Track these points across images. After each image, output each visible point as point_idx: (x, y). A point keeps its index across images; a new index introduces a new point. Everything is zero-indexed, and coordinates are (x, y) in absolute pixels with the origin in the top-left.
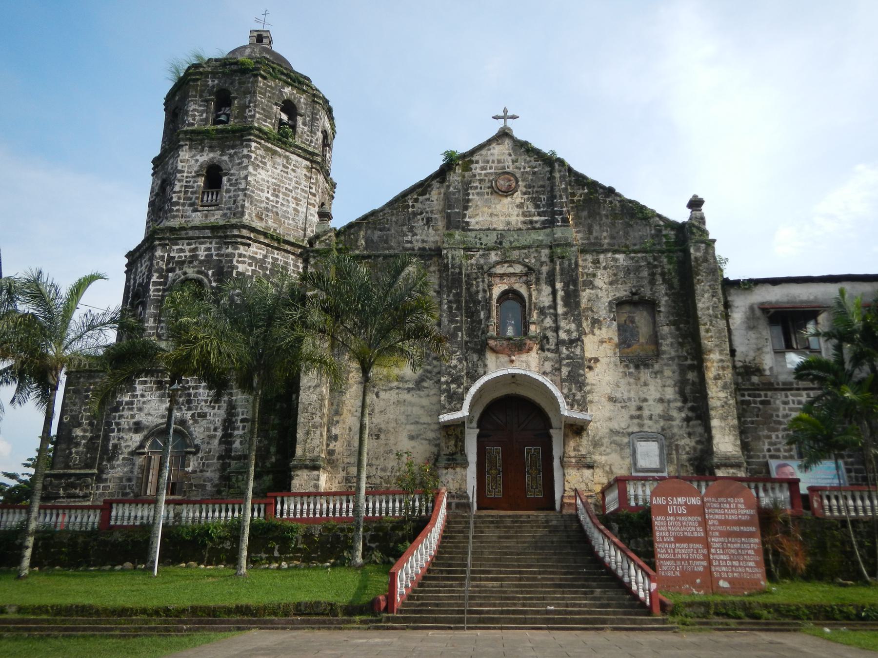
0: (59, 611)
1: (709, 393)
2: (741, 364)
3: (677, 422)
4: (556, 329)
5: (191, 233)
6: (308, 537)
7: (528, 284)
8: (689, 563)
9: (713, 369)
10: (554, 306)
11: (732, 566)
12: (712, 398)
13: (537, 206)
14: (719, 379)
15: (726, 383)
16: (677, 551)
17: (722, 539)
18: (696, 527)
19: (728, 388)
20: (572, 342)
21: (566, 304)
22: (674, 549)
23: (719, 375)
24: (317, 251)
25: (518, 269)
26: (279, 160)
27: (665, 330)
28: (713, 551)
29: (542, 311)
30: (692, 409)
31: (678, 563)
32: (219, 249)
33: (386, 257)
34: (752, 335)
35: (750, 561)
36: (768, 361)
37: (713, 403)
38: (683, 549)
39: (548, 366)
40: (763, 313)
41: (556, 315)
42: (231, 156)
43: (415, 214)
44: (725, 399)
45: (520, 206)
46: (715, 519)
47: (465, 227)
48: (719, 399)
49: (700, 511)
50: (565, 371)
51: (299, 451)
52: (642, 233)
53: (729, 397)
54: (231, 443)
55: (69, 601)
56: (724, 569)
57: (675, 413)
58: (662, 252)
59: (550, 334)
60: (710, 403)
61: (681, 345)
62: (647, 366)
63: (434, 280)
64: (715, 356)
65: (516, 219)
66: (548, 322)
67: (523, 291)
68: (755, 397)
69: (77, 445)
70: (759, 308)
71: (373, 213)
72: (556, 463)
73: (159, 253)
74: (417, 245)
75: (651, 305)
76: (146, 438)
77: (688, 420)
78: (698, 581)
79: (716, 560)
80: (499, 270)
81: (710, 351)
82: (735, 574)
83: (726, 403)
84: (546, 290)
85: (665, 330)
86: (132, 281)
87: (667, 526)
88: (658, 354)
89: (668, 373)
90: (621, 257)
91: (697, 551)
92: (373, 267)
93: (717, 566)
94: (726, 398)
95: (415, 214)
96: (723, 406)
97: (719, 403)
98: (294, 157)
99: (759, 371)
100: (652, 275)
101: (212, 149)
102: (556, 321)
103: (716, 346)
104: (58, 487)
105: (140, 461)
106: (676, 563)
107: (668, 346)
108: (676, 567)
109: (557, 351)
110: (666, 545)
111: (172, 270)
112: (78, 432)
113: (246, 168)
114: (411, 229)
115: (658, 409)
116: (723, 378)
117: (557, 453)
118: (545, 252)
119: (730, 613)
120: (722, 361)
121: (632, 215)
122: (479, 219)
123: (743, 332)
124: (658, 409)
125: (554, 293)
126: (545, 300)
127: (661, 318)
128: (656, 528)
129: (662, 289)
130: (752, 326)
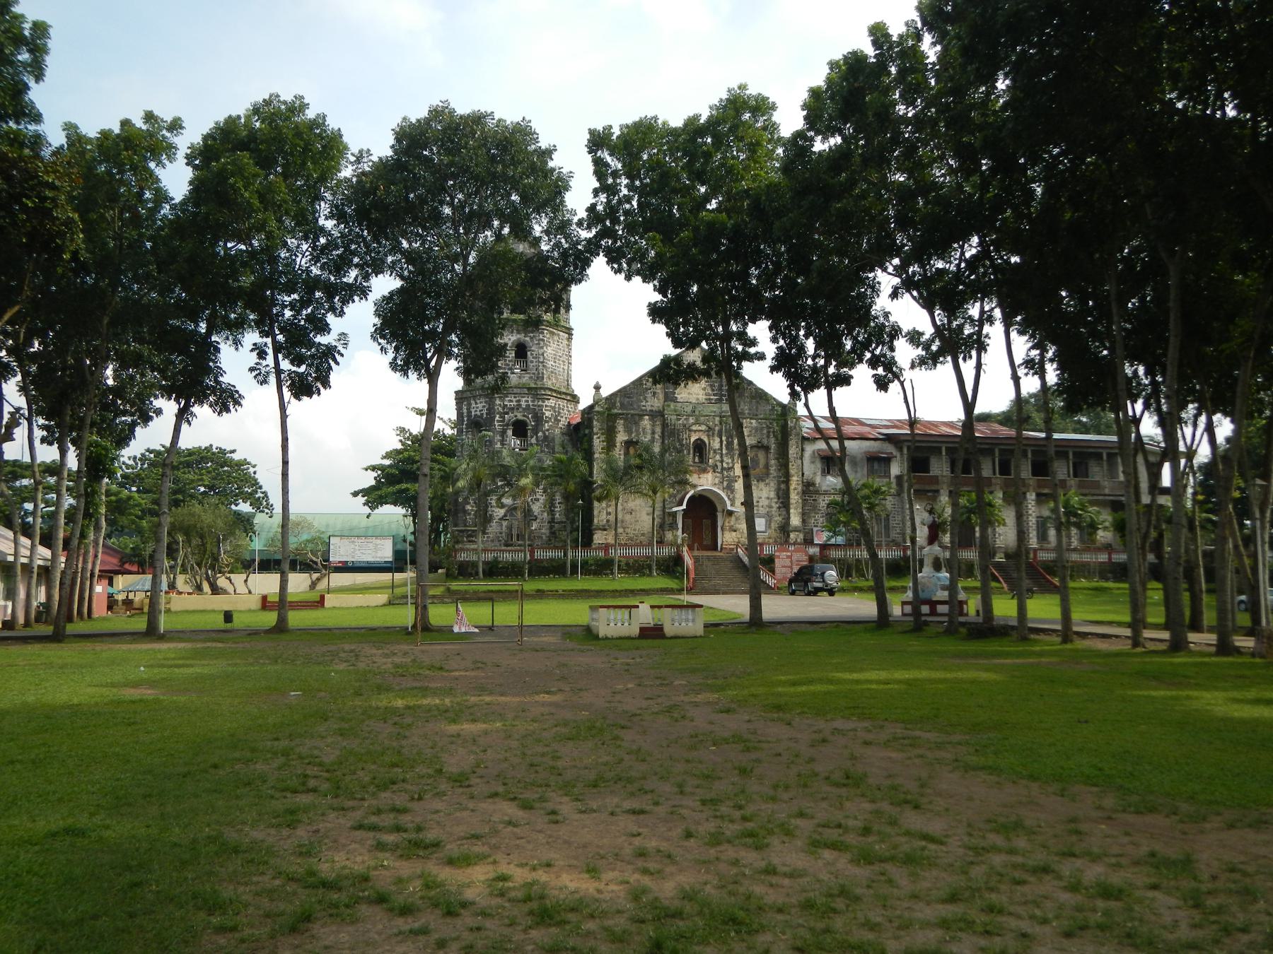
0: (577, 591)
3: (774, 509)
4: (722, 462)
5: (515, 391)
6: (627, 564)
7: (708, 436)
10: (721, 449)
13: (713, 390)
20: (729, 469)
21: (727, 449)
24: (598, 412)
25: (703, 427)
26: (556, 338)
27: (773, 462)
29: (715, 451)
30: (782, 503)
32: (533, 401)
33: (632, 415)
34: (813, 466)
36: (818, 480)
37: (792, 501)
38: (784, 570)
39: (717, 481)
41: (722, 454)
42: (531, 338)
43: (647, 389)
45: (704, 389)
47: (675, 400)
49: (790, 557)
50: (725, 483)
51: (596, 521)
52: (765, 409)
54: (554, 515)
55: (580, 588)
57: (773, 505)
58: (774, 420)
59: (719, 464)
61: (780, 470)
62: (763, 481)
63: (658, 430)
64: (795, 478)
65: (702, 397)
66: (718, 457)
67: (706, 440)
69: (469, 514)
71: (625, 388)
72: (719, 529)
73: (498, 402)
74: (649, 408)
75: (767, 449)
76: (507, 511)
77: (779, 508)
80: (694, 428)
84: (717, 440)
85: (773, 462)
86: (465, 411)
88: (768, 474)
89: (772, 484)
90: (754, 421)
92: (625, 420)
95: (647, 389)
98: (561, 333)
99: (813, 484)
100: (769, 432)
101: (518, 332)
102: (722, 457)
104: (463, 537)
105: (505, 523)
107: (773, 470)
109: (722, 473)
111: (507, 413)
112: (469, 507)
113: (542, 348)
114: (645, 398)
115: (766, 503)
117: (720, 524)
118: (717, 419)
121: (761, 398)
122: (682, 395)
124: (766, 503)
125: (721, 442)
126: (716, 445)
127: (771, 456)
129: (773, 440)
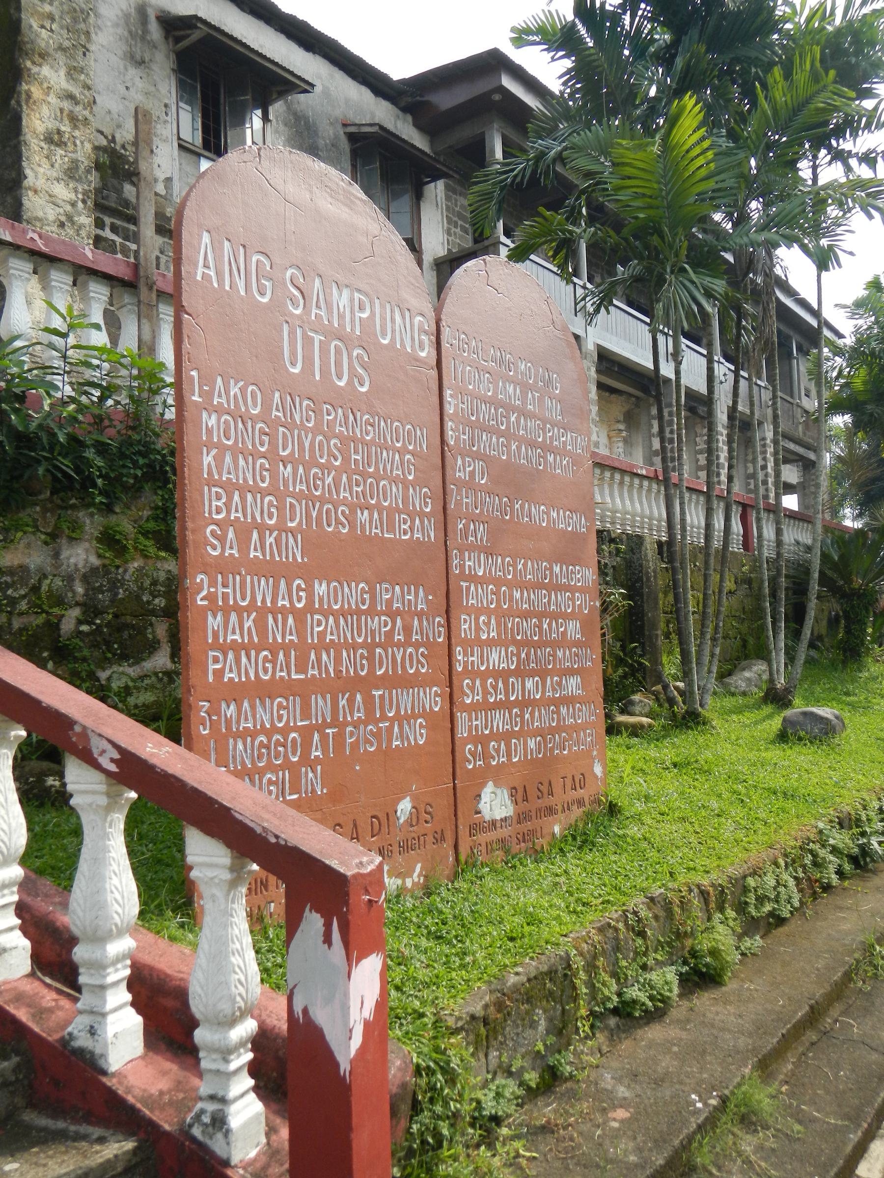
1: (28, 172)
2: (104, 142)
8: (369, 701)
9: (45, 111)
11: (525, 703)
12: (36, 191)
14: (57, 145)
15: (75, 162)
16: (317, 626)
17: (497, 566)
18: (406, 484)
19: (79, 180)
22: (300, 616)
23: (59, 132)
28: (465, 626)
31: (320, 705)
35: (571, 672)
40: (166, 38)
44: (68, 208)
46: (478, 456)
48: (52, 199)
53: (80, 205)
56: (499, 721)
60: (25, 201)
68: (126, 238)
70: (158, 18)
78: (405, 807)
79: (472, 674)
81: (43, 56)
82: (532, 744)
83: (70, 218)
87: (272, 456)
91: (407, 630)
93: (475, 708)
94: (73, 204)
96: (62, 225)
97: (51, 213)
103: (61, 48)
106: (306, 713)
108: (306, 733)
110: (262, 592)
116: (71, 147)
119: (634, 993)
120: (71, 97)
123: (116, 61)
128: (208, 459)
130: (138, 57)
